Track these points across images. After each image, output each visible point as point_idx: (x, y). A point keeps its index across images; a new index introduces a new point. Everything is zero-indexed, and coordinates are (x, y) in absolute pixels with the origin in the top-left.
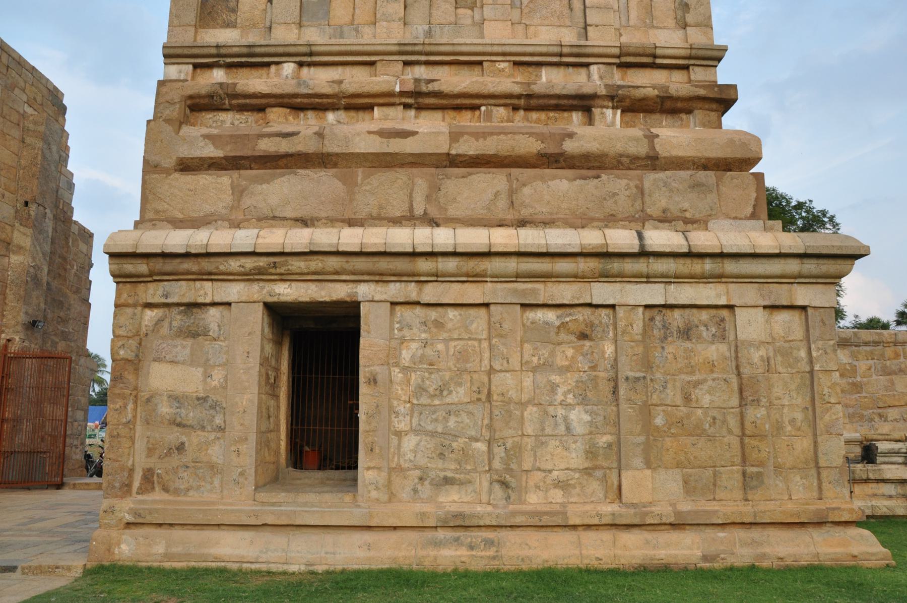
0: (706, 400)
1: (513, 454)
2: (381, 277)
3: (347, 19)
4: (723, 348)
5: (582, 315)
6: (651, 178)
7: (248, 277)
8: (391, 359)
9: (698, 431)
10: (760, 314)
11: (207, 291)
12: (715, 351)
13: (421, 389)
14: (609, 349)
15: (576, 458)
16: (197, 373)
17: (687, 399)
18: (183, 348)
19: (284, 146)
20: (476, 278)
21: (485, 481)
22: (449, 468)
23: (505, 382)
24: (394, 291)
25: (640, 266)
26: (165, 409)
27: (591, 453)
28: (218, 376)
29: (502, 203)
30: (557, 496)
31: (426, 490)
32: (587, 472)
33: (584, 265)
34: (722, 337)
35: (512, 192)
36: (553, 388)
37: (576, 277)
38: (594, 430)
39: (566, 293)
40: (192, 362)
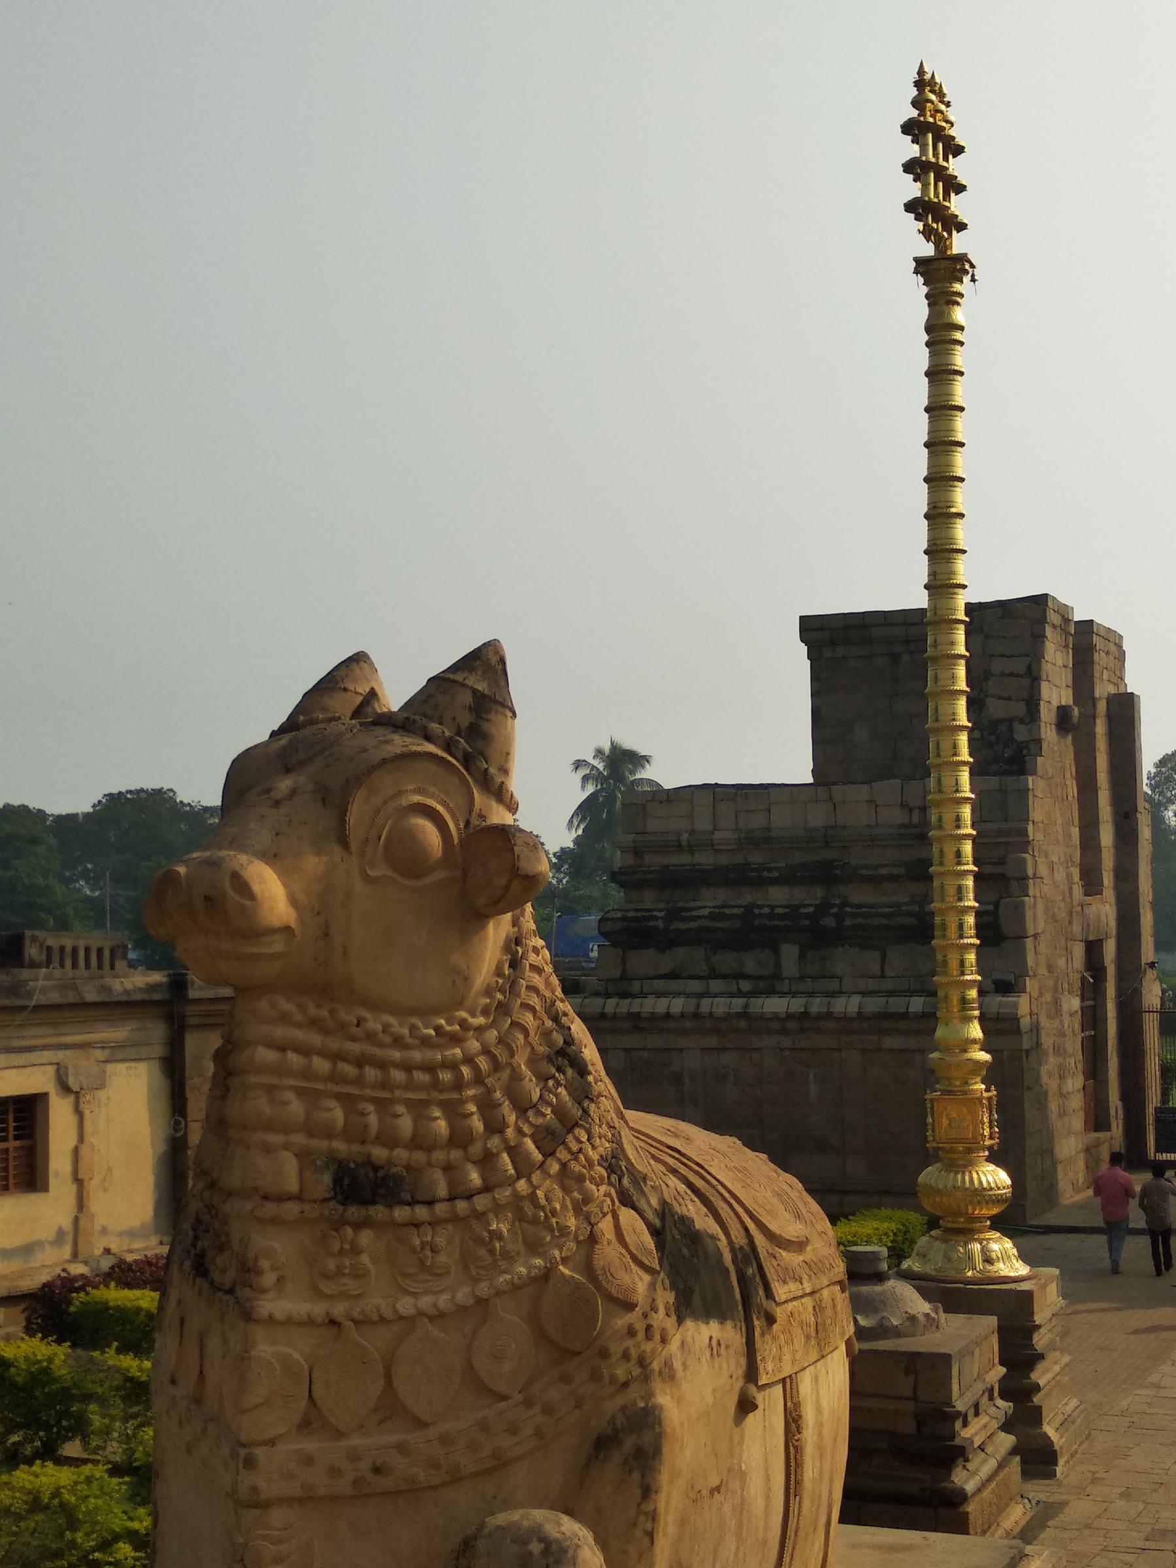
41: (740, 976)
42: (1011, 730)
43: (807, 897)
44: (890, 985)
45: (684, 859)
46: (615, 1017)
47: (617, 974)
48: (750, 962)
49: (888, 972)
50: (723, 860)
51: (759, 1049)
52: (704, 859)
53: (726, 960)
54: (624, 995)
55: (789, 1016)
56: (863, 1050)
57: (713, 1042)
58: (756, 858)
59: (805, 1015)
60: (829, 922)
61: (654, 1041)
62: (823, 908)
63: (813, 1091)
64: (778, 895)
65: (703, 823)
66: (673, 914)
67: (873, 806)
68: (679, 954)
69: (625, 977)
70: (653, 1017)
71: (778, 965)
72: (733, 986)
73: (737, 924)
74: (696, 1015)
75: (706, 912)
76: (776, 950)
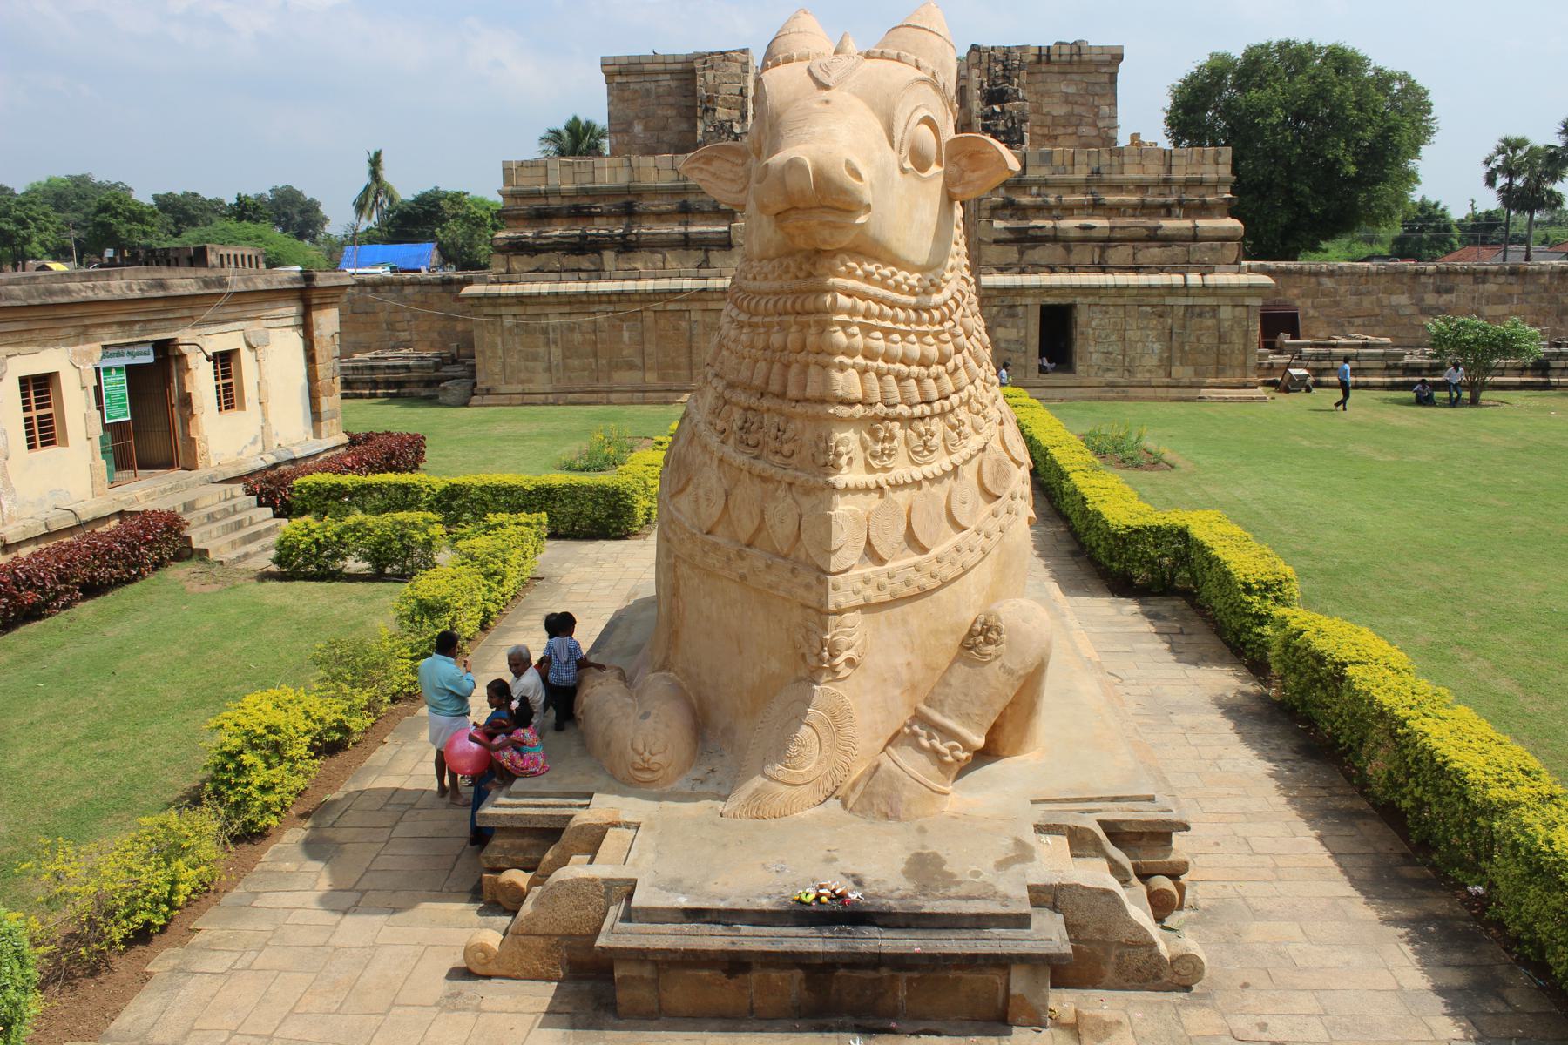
0: (1206, 341)
1: (1133, 359)
2: (1086, 296)
3: (1060, 163)
4: (1214, 321)
5: (1160, 309)
6: (1193, 245)
7: (1034, 296)
8: (1088, 325)
9: (1202, 352)
10: (1229, 308)
11: (1019, 300)
12: (1210, 322)
13: (1099, 336)
14: (1170, 321)
15: (1155, 361)
16: (1015, 331)
17: (1198, 340)
18: (1009, 322)
19: (1039, 233)
20: (1121, 296)
21: (1120, 370)
22: (1108, 365)
23: (1132, 334)
24: (1090, 300)
25: (1185, 291)
26: (1003, 345)
27: (1161, 360)
28: (1022, 333)
29: (1131, 258)
30: (1148, 375)
31: (1100, 373)
32: (1159, 367)
33: (1162, 291)
34: (1214, 316)
35: (1134, 254)
36: (1148, 336)
37: (1159, 295)
38: (1162, 351)
39: (1155, 301)
40: (1013, 327)
42: (731, 126)
45: (542, 201)
47: (503, 270)
48: (585, 262)
49: (668, 266)
50: (566, 203)
52: (555, 202)
54: (510, 283)
57: (567, 309)
58: (585, 202)
61: (530, 310)
63: (626, 335)
66: (538, 236)
68: (542, 258)
69: (508, 272)
70: (530, 296)
71: (602, 263)
73: (578, 239)
74: (557, 294)
76: (600, 254)
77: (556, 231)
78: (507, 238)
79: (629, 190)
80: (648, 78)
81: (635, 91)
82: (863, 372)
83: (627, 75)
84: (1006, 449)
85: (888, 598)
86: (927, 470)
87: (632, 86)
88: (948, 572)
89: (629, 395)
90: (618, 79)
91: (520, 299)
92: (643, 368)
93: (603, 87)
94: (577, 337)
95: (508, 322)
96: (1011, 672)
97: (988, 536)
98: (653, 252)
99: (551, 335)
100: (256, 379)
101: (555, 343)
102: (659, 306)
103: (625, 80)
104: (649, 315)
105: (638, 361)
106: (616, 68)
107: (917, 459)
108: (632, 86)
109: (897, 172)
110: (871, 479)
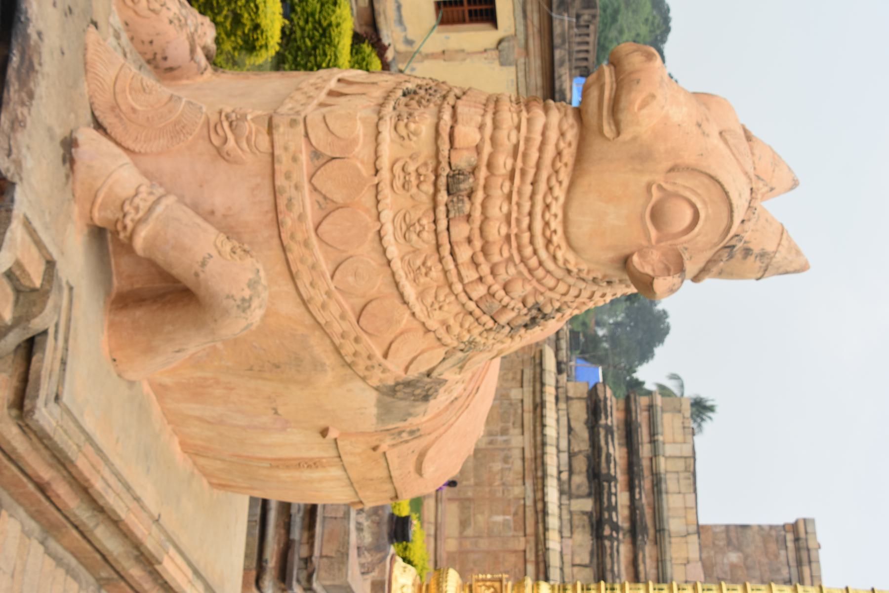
41: (571, 472)
43: (621, 517)
44: (567, 570)
46: (542, 392)
47: (571, 394)
48: (580, 479)
49: (576, 569)
50: (645, 463)
51: (524, 484)
52: (645, 451)
53: (581, 464)
54: (557, 399)
55: (545, 504)
56: (525, 551)
57: (528, 454)
58: (647, 484)
59: (545, 513)
60: (607, 531)
62: (615, 527)
63: (499, 518)
64: (622, 499)
65: (669, 450)
66: (609, 430)
67: (685, 562)
69: (568, 399)
71: (579, 497)
72: (564, 467)
73: (604, 471)
74: (544, 444)
75: (611, 451)
76: (589, 495)
77: (617, 451)
78: (606, 399)
79: (660, 531)
80: (794, 570)
81: (777, 556)
82: (478, 149)
83: (798, 550)
84: (402, 333)
85: (278, 183)
86: (388, 229)
87: (783, 552)
88: (296, 251)
89: (432, 520)
90: (790, 537)
91: (539, 406)
92: (462, 537)
93: (780, 521)
94: (497, 466)
95: (515, 394)
96: (203, 264)
97: (324, 306)
98: (592, 554)
99: (500, 438)
100: (468, 47)
101: (491, 442)
102: (531, 556)
103: (790, 545)
104: (520, 544)
105: (469, 532)
106: (802, 535)
107: (401, 215)
108: (783, 552)
109: (646, 179)
110: (385, 163)
